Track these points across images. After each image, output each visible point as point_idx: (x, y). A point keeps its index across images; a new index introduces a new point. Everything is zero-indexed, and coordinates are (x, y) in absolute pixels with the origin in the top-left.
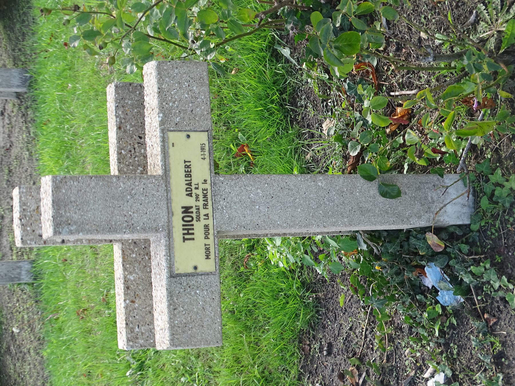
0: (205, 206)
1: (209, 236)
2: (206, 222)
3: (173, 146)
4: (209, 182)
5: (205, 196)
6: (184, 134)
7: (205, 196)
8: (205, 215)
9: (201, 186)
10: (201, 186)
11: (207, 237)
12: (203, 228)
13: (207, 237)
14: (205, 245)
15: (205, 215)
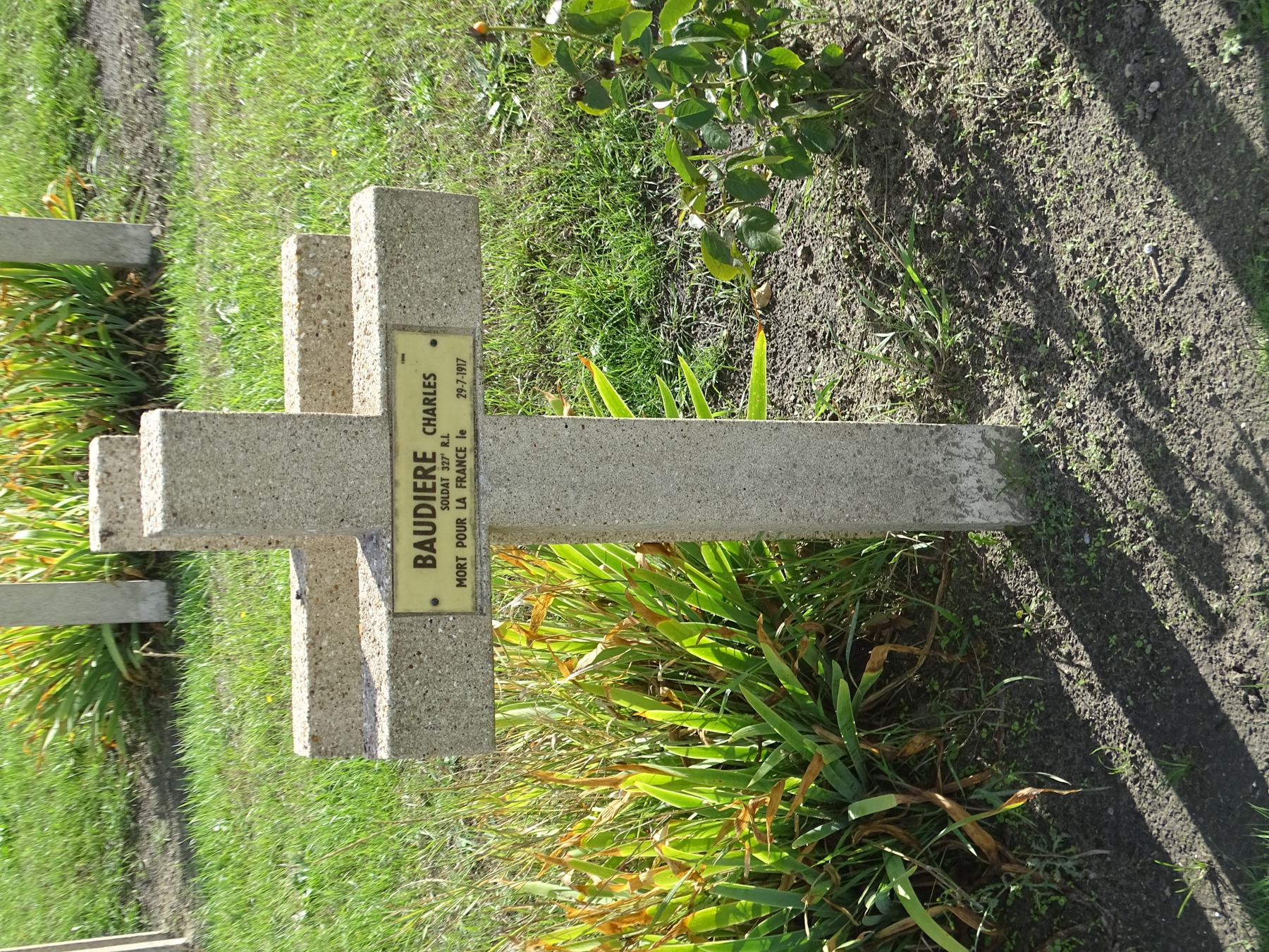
0: (460, 482)
1: (465, 542)
2: (464, 514)
3: (403, 359)
4: (470, 434)
5: (461, 463)
6: (427, 339)
7: (461, 463)
8: (458, 500)
9: (455, 443)
10: (455, 443)
11: (460, 544)
12: (454, 524)
13: (460, 544)
14: (457, 559)
15: (458, 500)
